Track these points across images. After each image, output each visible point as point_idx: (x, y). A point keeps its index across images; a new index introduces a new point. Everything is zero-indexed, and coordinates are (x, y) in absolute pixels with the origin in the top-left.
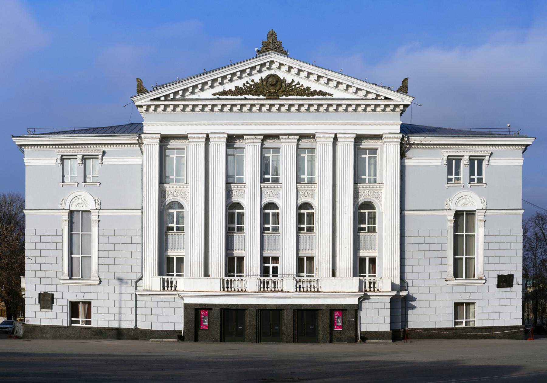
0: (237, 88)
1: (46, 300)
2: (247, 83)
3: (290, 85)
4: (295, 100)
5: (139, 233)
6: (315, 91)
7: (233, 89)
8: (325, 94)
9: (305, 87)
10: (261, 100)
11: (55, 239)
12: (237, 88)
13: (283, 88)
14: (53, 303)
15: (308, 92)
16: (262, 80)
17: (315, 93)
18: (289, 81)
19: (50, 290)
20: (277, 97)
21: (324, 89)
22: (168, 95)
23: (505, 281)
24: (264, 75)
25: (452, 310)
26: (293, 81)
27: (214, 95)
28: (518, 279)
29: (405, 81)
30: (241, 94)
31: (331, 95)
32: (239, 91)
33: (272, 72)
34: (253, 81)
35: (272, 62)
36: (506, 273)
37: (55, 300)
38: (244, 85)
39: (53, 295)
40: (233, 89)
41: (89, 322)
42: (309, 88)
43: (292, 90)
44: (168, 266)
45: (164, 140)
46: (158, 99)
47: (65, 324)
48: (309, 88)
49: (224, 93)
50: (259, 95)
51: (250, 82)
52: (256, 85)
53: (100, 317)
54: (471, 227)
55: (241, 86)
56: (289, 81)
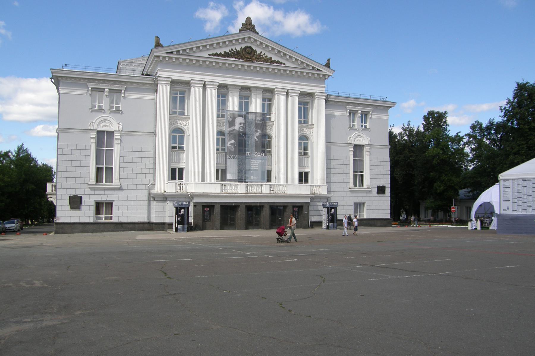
0: (225, 52)
1: (75, 202)
2: (232, 49)
3: (259, 55)
4: (261, 64)
5: (152, 150)
6: (275, 60)
7: (223, 53)
8: (281, 63)
9: (269, 57)
10: (241, 62)
11: (83, 153)
12: (225, 52)
13: (255, 56)
14: (81, 203)
15: (270, 61)
16: (242, 50)
17: (275, 62)
18: (258, 52)
19: (78, 193)
20: (252, 61)
21: (280, 60)
22: (179, 51)
23: (381, 190)
24: (243, 46)
25: (352, 208)
26: (261, 52)
27: (209, 55)
28: (388, 190)
29: (329, 60)
30: (228, 57)
31: (285, 64)
32: (226, 55)
33: (249, 45)
34: (236, 49)
35: (249, 38)
36: (381, 185)
37: (83, 201)
38: (230, 51)
39: (81, 197)
40: (223, 53)
41: (111, 218)
42: (271, 58)
43: (261, 58)
44: (176, 174)
45: (174, 82)
46: (171, 53)
47: (92, 220)
48: (271, 58)
49: (216, 55)
50: (240, 59)
51: (234, 49)
52: (237, 52)
53: (120, 214)
54: (361, 156)
55: (228, 51)
56: (258, 52)
